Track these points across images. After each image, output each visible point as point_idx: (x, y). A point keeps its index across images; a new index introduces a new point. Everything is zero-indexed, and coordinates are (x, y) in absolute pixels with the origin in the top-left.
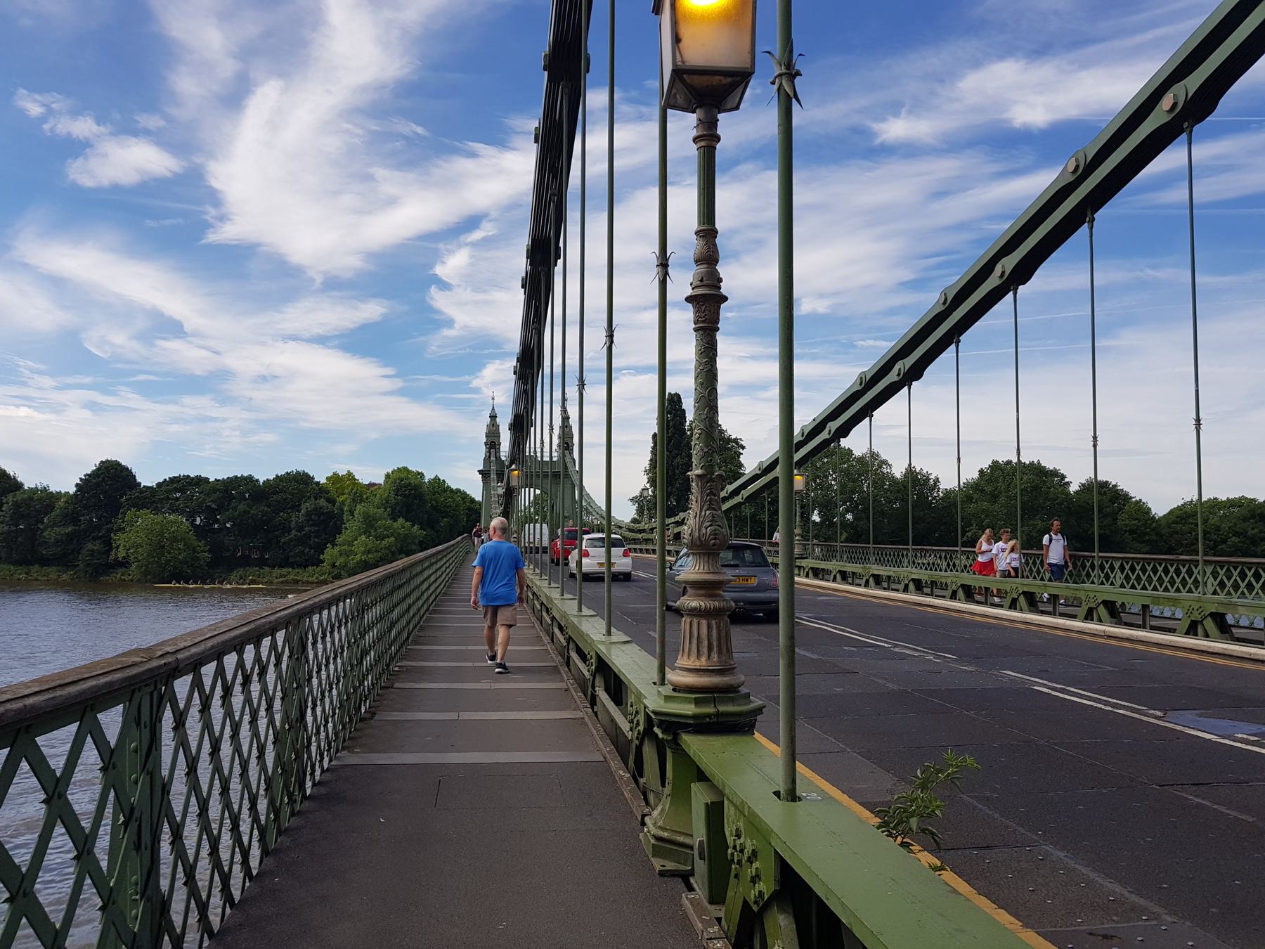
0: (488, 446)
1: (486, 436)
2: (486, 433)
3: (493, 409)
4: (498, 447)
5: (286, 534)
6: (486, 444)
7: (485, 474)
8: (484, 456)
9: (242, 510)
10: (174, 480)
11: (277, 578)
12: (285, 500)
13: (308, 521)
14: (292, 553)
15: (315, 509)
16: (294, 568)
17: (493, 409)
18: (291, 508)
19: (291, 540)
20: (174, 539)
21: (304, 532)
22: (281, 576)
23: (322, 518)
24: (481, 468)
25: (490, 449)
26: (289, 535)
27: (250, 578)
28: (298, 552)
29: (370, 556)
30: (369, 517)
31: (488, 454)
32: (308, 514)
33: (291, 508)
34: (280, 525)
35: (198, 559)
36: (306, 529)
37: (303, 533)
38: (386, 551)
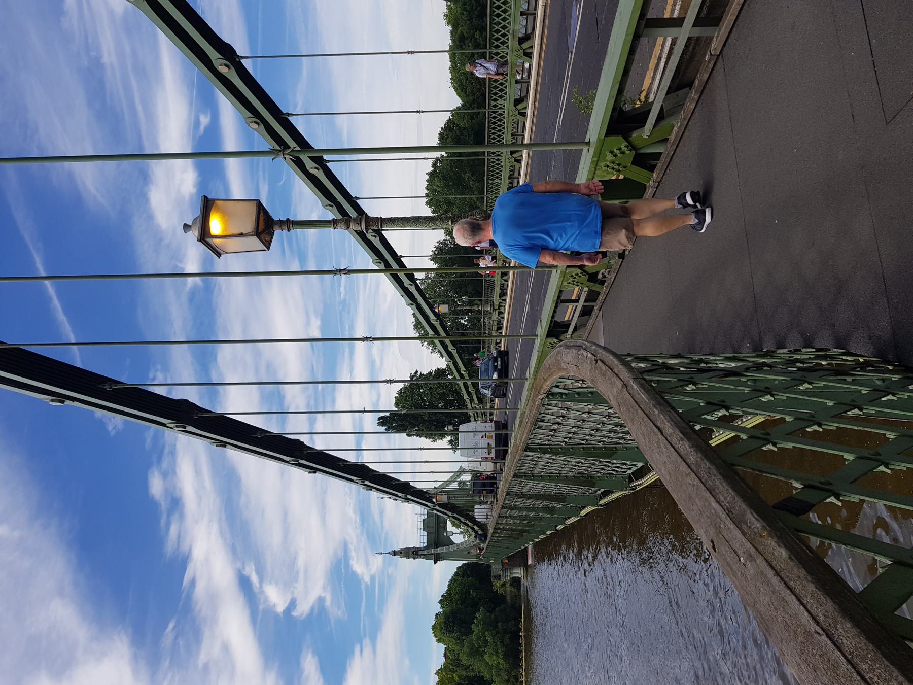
0: (416, 557)
1: (409, 558)
2: (407, 558)
3: (389, 553)
4: (417, 549)
6: (415, 558)
7: (437, 558)
8: (424, 560)
17: (389, 553)
24: (432, 561)
25: (419, 555)
29: (499, 651)
31: (422, 556)
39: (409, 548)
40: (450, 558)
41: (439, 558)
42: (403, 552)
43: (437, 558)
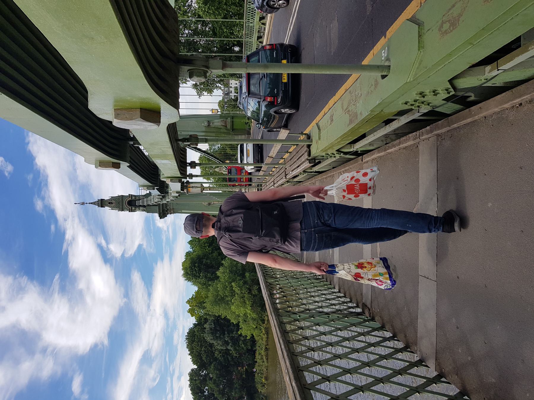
0: (133, 208)
2: (119, 210)
3: (94, 203)
4: (133, 198)
5: (231, 352)
6: (131, 211)
9: (213, 385)
11: (264, 362)
12: (205, 352)
13: (220, 338)
14: (245, 348)
15: (212, 333)
16: (256, 350)
17: (94, 203)
18: (211, 348)
19: (235, 349)
22: (262, 359)
23: (218, 328)
25: (136, 206)
26: (231, 350)
27: (263, 380)
28: (244, 344)
29: (247, 302)
30: (215, 301)
31: (141, 208)
32: (216, 338)
33: (211, 348)
34: (223, 356)
36: (227, 340)
37: (229, 341)
40: (183, 211)
41: (167, 211)
42: (113, 201)
43: (163, 210)
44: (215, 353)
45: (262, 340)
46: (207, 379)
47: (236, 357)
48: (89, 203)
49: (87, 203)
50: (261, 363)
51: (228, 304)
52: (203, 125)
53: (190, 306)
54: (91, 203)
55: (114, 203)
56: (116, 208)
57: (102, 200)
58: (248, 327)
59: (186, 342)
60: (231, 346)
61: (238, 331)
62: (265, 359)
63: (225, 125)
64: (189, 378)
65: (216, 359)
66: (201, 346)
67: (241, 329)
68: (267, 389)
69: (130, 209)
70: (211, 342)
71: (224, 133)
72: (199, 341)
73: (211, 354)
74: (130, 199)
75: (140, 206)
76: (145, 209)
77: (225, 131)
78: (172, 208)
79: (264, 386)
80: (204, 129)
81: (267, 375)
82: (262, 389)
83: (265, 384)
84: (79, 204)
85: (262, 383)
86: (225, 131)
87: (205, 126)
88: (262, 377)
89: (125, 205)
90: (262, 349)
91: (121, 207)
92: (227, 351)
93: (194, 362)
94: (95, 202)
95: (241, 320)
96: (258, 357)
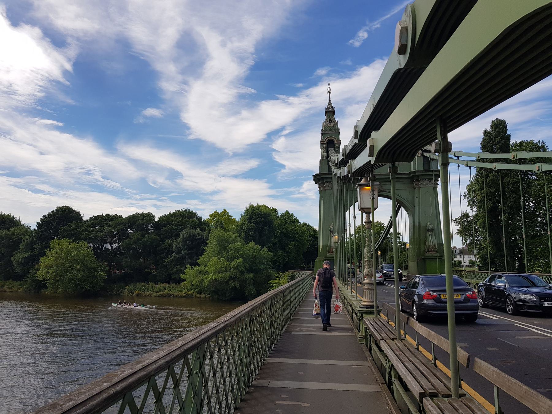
0: (325, 146)
1: (322, 134)
2: (322, 130)
4: (337, 145)
5: (169, 256)
6: (322, 143)
9: (136, 238)
10: (96, 218)
11: (156, 292)
12: (172, 229)
15: (190, 237)
16: (169, 284)
18: (175, 236)
20: (76, 261)
21: (181, 254)
22: (160, 290)
23: (194, 243)
26: (171, 257)
28: (177, 270)
29: (220, 275)
30: (222, 240)
31: (325, 154)
32: (184, 240)
34: (165, 249)
35: (96, 277)
36: (182, 252)
38: (235, 271)
39: (339, 133)
40: (322, 201)
41: (322, 183)
42: (332, 124)
43: (323, 179)
44: (169, 239)
45: (180, 291)
46: (143, 232)
47: (164, 262)
48: (330, 99)
49: (329, 96)
50: (155, 290)
51: (219, 253)
52: (428, 223)
53: (221, 214)
54: (330, 101)
55: (330, 125)
56: (325, 127)
57: (334, 112)
58: (193, 276)
59: (183, 209)
60: (175, 257)
61: (190, 265)
62: (159, 294)
63: (430, 250)
64: (146, 213)
65: (163, 240)
66: (177, 225)
67: (192, 267)
68: (128, 295)
69: (324, 142)
70: (181, 236)
71: (419, 249)
72: (182, 223)
73: (168, 235)
74: (336, 142)
75: (328, 153)
76: (324, 158)
77: (422, 250)
78: (326, 188)
79: (131, 293)
80: (422, 224)
81: (142, 296)
82: (128, 290)
83: (133, 293)
84: (329, 88)
85: (134, 290)
86: (422, 250)
87: (426, 226)
88: (140, 290)
89: (328, 137)
90: (170, 290)
91: (326, 132)
92: (170, 253)
93: (161, 219)
94: (331, 105)
95: (202, 267)
96: (161, 286)
